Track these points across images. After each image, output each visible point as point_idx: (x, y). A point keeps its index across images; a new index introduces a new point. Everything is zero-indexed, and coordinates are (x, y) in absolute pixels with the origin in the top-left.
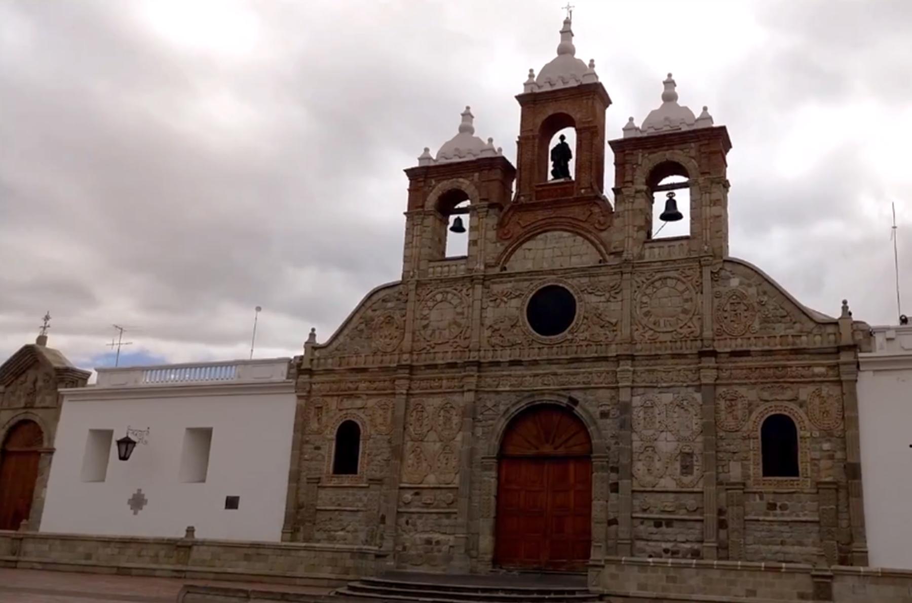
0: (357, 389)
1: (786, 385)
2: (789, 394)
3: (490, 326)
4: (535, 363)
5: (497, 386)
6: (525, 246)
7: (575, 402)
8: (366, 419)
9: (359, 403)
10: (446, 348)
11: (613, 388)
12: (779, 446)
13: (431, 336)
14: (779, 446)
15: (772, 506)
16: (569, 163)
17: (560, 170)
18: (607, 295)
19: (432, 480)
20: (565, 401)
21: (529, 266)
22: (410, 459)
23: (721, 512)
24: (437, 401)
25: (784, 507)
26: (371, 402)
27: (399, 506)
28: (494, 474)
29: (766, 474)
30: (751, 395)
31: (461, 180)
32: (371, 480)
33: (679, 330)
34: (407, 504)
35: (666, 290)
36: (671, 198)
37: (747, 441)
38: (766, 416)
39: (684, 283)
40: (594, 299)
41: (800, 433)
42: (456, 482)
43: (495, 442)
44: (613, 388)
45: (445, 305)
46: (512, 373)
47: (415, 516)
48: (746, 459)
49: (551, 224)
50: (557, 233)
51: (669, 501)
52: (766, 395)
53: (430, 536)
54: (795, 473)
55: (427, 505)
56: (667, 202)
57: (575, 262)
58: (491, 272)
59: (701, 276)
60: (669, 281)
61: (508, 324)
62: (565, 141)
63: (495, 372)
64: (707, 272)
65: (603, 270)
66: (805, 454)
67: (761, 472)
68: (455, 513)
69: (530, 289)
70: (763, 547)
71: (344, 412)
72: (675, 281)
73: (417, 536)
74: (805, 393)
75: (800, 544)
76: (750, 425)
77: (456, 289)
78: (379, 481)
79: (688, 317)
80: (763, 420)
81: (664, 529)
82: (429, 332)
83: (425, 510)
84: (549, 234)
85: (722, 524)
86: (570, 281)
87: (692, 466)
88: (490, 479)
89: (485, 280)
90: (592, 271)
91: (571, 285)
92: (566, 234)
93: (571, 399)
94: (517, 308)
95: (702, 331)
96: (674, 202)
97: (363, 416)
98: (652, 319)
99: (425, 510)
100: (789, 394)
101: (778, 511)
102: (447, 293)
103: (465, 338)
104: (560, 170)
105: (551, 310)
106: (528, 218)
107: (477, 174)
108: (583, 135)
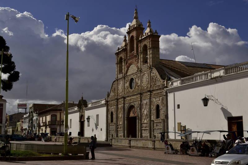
7: (135, 104)
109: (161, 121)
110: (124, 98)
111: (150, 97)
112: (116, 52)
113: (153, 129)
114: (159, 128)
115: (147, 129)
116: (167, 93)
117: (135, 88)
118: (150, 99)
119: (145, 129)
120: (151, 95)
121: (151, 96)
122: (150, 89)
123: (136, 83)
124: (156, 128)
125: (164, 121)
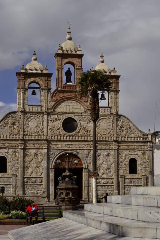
0: (4, 146)
1: (135, 150)
2: (136, 153)
3: (50, 129)
4: (66, 141)
5: (54, 147)
7: (78, 153)
8: (9, 156)
9: (6, 150)
10: (36, 134)
11: (89, 150)
12: (133, 166)
13: (30, 130)
14: (133, 166)
15: (131, 182)
16: (71, 77)
17: (68, 80)
18: (87, 122)
20: (75, 153)
21: (61, 110)
24: (34, 151)
26: (10, 150)
29: (129, 174)
30: (127, 152)
31: (37, 79)
32: (12, 175)
33: (107, 134)
35: (104, 122)
36: (103, 93)
37: (125, 165)
38: (130, 159)
39: (109, 120)
40: (82, 123)
41: (138, 163)
44: (89, 150)
45: (34, 120)
46: (58, 143)
47: (28, 186)
49: (69, 98)
50: (71, 101)
51: (105, 181)
52: (130, 153)
53: (34, 191)
54: (136, 173)
55: (32, 182)
56: (102, 95)
57: (77, 111)
58: (50, 111)
59: (113, 119)
60: (105, 119)
61: (56, 128)
62: (70, 70)
63: (52, 143)
64: (115, 118)
65: (86, 114)
66: (139, 168)
67: (128, 172)
68: (43, 185)
69: (63, 118)
72: (106, 120)
74: (140, 153)
76: (126, 160)
77: (37, 115)
79: (110, 130)
80: (129, 159)
81: (104, 188)
82: (29, 129)
83: (32, 184)
84: (68, 101)
86: (75, 116)
87: (111, 171)
89: (48, 114)
90: (82, 114)
91: (76, 118)
93: (77, 152)
94: (59, 124)
95: (113, 135)
96: (104, 95)
97: (7, 154)
98: (100, 130)
99: (32, 184)
100: (136, 153)
101: (133, 183)
102: (35, 116)
103: (42, 132)
104: (68, 80)
105: (69, 125)
106: (61, 95)
107: (42, 78)
108: (78, 71)
109: (140, 176)
110: (49, 142)
111: (118, 148)
112: (19, 72)
113: (125, 186)
114: (136, 184)
115: (109, 186)
116: (152, 147)
117: (79, 132)
118: (118, 150)
119: (103, 185)
120: (119, 146)
121: (119, 147)
122: (116, 139)
123: (81, 126)
124: (130, 185)
125: (147, 178)
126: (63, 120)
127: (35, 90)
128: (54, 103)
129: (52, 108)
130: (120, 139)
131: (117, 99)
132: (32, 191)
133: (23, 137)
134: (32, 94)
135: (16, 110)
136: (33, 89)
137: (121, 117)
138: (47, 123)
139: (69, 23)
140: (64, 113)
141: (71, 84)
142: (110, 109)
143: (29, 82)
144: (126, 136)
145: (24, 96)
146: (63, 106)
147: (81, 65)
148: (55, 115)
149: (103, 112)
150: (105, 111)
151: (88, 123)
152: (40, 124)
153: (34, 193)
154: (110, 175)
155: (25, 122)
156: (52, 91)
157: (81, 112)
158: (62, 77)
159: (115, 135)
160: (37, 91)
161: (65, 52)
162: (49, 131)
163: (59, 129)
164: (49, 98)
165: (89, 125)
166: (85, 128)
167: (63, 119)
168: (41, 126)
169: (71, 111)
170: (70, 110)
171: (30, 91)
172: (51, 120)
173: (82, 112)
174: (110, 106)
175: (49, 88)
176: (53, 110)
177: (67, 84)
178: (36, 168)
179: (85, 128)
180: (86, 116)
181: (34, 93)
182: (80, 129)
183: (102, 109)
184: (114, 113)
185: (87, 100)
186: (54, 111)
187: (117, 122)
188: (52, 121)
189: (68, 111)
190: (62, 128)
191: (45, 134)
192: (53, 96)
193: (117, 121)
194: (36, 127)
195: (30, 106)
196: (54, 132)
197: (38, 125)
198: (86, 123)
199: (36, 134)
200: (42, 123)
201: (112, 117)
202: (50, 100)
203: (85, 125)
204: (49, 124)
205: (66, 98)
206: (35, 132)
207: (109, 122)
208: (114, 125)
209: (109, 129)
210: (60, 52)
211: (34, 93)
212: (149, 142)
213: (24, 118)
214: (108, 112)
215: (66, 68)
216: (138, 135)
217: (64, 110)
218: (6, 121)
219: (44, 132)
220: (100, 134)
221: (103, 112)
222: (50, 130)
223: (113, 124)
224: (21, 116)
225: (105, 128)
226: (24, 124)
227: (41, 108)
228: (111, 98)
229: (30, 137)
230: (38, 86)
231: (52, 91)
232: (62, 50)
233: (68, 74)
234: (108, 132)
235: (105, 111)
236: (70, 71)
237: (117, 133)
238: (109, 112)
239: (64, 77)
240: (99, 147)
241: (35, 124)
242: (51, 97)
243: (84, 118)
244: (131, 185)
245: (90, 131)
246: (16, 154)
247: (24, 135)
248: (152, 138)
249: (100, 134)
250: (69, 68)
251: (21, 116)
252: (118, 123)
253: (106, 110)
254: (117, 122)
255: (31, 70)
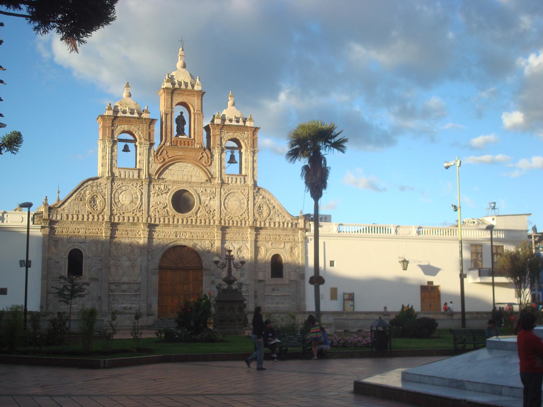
6: (170, 168)
15: (274, 290)
17: (181, 131)
19: (125, 279)
22: (113, 269)
23: (255, 292)
25: (278, 290)
27: (109, 292)
28: (157, 276)
31: (133, 127)
34: (112, 291)
42: (139, 280)
43: (157, 261)
48: (265, 271)
49: (182, 159)
50: (185, 164)
55: (124, 291)
57: (194, 179)
59: (249, 194)
61: (161, 206)
69: (174, 189)
70: (270, 305)
71: (72, 244)
73: (119, 305)
75: (283, 303)
78: (96, 280)
79: (244, 211)
83: (122, 294)
84: (181, 164)
85: (256, 297)
88: (155, 279)
92: (190, 165)
94: (167, 199)
97: (84, 246)
99: (122, 294)
104: (181, 131)
105: (181, 202)
109: (287, 282)
123: (200, 204)
126: (173, 193)
127: (128, 144)
128: (159, 166)
129: (156, 174)
130: (258, 225)
131: (255, 164)
132: (124, 305)
133: (110, 218)
134: (123, 151)
135: (99, 174)
136: (125, 143)
137: (261, 190)
138: (149, 197)
139: (182, 41)
140: (174, 182)
141: (186, 137)
142: (244, 179)
143: (120, 132)
144: (267, 221)
145: (112, 153)
146: (173, 172)
147: (202, 108)
148: (160, 185)
149: (234, 182)
150: (236, 182)
151: (211, 199)
152: (137, 198)
153: (125, 308)
154: (243, 278)
155: (113, 195)
156: (155, 148)
157: (200, 181)
158: (171, 125)
159: (251, 220)
160: (131, 146)
161: (177, 86)
162: (152, 209)
163: (164, 208)
164: (151, 160)
165: (212, 202)
166: (207, 206)
167: (172, 192)
168: (139, 202)
169: (185, 180)
170: (183, 178)
171: (121, 145)
172: (154, 192)
173: (203, 181)
174: (243, 173)
175: (152, 142)
176: (157, 176)
177: (180, 137)
178: (130, 268)
179: (207, 206)
180: (207, 187)
181: (126, 149)
182: (199, 208)
183: (232, 178)
184: (250, 185)
185: (209, 163)
186: (158, 178)
187: (254, 199)
188: (156, 195)
189: (180, 178)
190: (172, 206)
191: (145, 215)
192: (157, 154)
193: (254, 197)
194: (131, 203)
195: (121, 170)
196: (158, 212)
197: (133, 201)
198: (209, 198)
199: (130, 215)
200: (139, 197)
201: (247, 191)
202: (152, 162)
203: (207, 202)
204: (152, 199)
205: (179, 159)
206: (129, 210)
207: (243, 199)
208: (249, 202)
209: (242, 208)
210: (169, 85)
211: (126, 149)
212: (301, 229)
213: (112, 188)
214: (241, 182)
215: (178, 111)
216: (284, 219)
217: (175, 179)
218: (82, 192)
219: (142, 210)
220: (228, 216)
221: (234, 182)
222: (153, 208)
223: (248, 200)
224: (106, 185)
225: (237, 207)
226: (111, 198)
227: (139, 173)
228: (246, 162)
229: (121, 218)
230: (130, 138)
231: (155, 148)
232: (173, 84)
233: (180, 121)
234: (241, 214)
235: (236, 182)
236: (183, 116)
237: (254, 215)
238: (242, 182)
239: (175, 126)
240: (228, 236)
241: (131, 199)
242: (154, 156)
243: (206, 190)
244: (273, 294)
245: (214, 210)
246: (97, 246)
247: (112, 214)
248: (305, 224)
249: (228, 216)
250: (182, 113)
251: (106, 185)
252: (256, 200)
253: (238, 180)
254: (254, 199)
255: (124, 112)
